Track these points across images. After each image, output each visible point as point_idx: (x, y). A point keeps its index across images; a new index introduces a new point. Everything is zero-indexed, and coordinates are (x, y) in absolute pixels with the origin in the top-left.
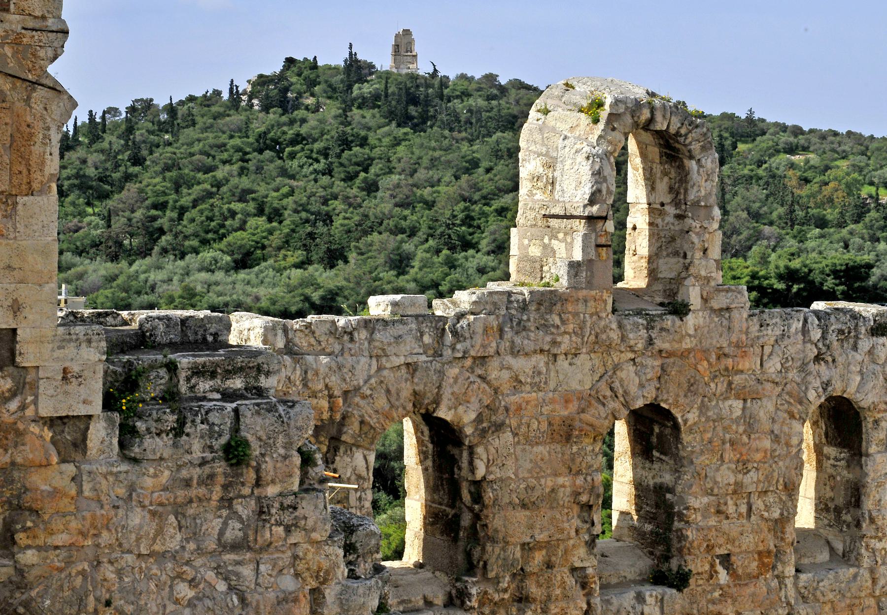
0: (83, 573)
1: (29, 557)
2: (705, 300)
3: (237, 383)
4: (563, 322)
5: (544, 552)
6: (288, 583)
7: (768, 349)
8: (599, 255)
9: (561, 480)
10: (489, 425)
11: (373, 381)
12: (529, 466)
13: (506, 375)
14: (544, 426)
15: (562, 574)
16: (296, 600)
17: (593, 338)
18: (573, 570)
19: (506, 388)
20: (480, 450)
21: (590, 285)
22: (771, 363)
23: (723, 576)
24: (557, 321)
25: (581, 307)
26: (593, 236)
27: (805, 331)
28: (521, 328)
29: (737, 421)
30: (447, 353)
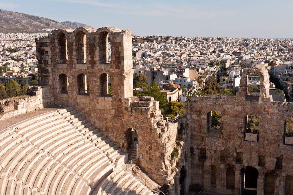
1: (123, 119)
2: (262, 99)
3: (145, 105)
6: (148, 127)
7: (275, 108)
9: (235, 123)
10: (223, 114)
12: (230, 120)
14: (232, 115)
15: (236, 136)
18: (239, 136)
21: (240, 96)
23: (267, 142)
24: (234, 100)
25: (238, 99)
29: (269, 119)
30: (216, 103)
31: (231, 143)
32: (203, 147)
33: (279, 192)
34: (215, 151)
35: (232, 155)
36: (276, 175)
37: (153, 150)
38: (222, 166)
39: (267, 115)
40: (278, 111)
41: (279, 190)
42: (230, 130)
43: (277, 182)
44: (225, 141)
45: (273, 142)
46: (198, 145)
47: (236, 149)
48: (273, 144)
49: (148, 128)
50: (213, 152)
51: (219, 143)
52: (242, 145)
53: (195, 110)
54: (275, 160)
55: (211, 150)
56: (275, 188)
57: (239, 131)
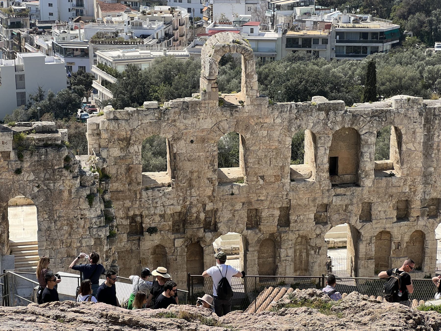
0: (11, 184)
2: (252, 102)
4: (201, 110)
5: (197, 173)
6: (61, 188)
8: (212, 90)
9: (201, 154)
11: (139, 127)
13: (182, 125)
16: (64, 192)
17: (211, 114)
18: (208, 179)
19: (182, 127)
20: (174, 145)
21: (210, 99)
22: (277, 120)
23: (261, 182)
26: (210, 85)
27: (290, 111)
28: (187, 112)
29: (265, 137)
30: (162, 119)
31: (194, 194)
32: (137, 213)
33: (286, 268)
34: (160, 216)
35: (197, 217)
36: (279, 240)
37: (75, 237)
38: (179, 243)
39: (261, 130)
40: (280, 121)
41: (286, 266)
42: (191, 170)
43: (283, 252)
44: (183, 192)
45: (273, 180)
46: (128, 209)
47: (204, 205)
48: (272, 183)
49: (61, 192)
50: (157, 218)
51: (168, 199)
52: (215, 195)
53: (116, 137)
54: (277, 213)
55: (155, 214)
56: (279, 264)
57: (208, 167)
